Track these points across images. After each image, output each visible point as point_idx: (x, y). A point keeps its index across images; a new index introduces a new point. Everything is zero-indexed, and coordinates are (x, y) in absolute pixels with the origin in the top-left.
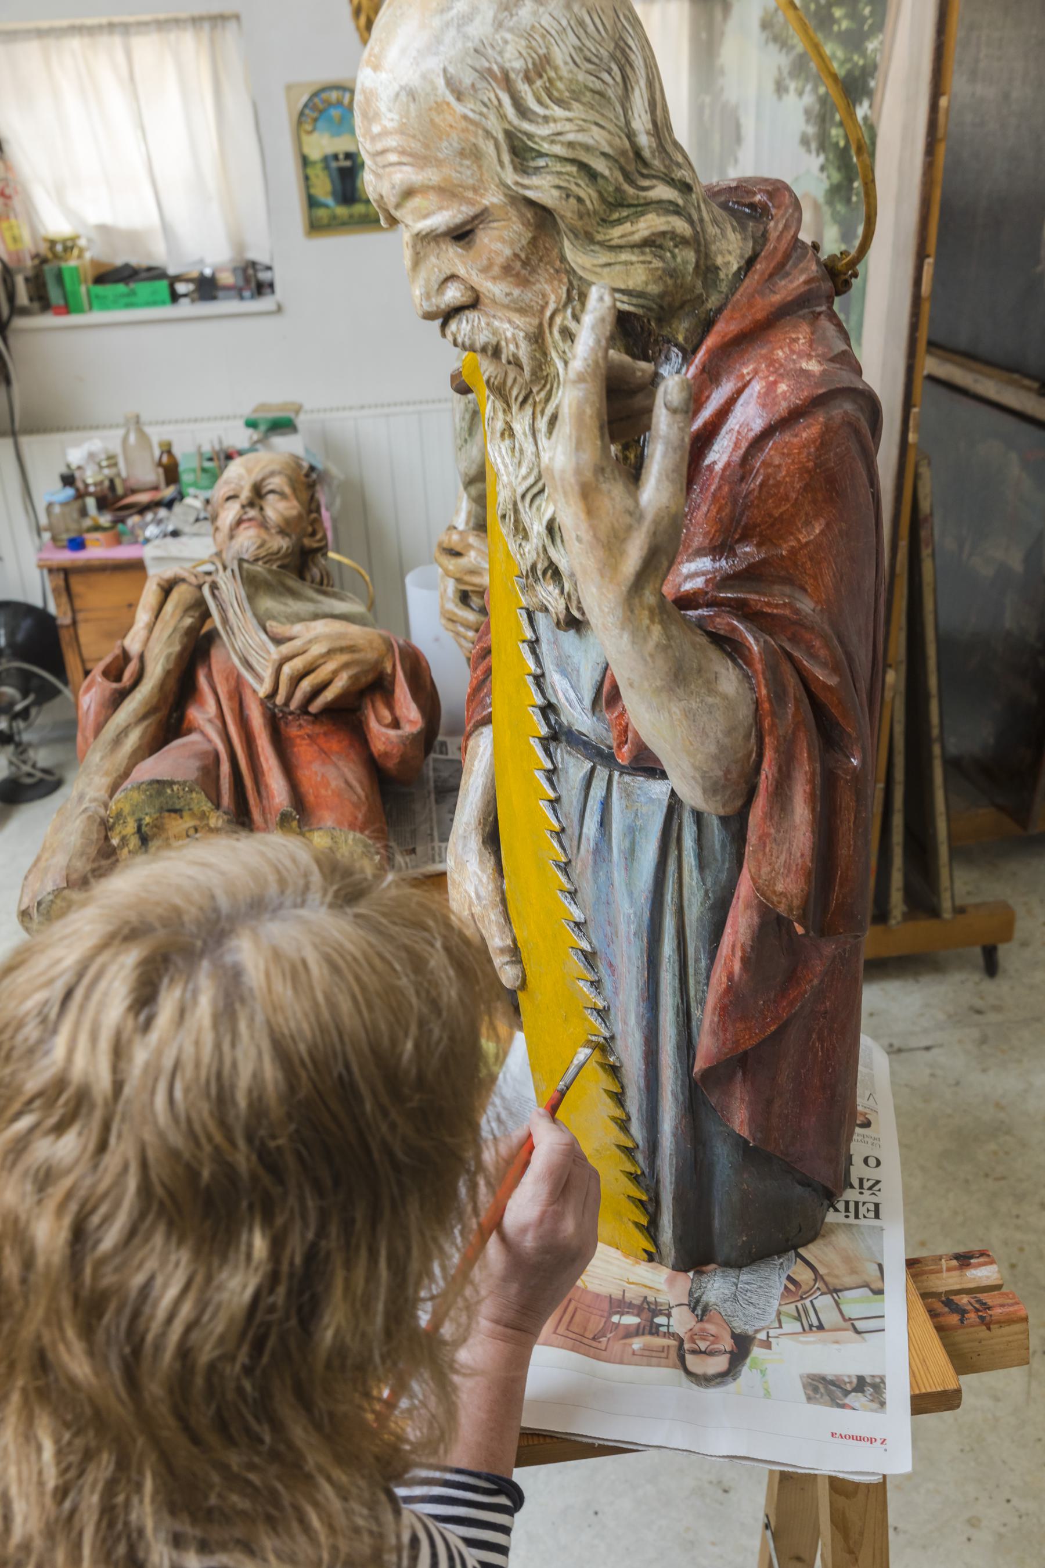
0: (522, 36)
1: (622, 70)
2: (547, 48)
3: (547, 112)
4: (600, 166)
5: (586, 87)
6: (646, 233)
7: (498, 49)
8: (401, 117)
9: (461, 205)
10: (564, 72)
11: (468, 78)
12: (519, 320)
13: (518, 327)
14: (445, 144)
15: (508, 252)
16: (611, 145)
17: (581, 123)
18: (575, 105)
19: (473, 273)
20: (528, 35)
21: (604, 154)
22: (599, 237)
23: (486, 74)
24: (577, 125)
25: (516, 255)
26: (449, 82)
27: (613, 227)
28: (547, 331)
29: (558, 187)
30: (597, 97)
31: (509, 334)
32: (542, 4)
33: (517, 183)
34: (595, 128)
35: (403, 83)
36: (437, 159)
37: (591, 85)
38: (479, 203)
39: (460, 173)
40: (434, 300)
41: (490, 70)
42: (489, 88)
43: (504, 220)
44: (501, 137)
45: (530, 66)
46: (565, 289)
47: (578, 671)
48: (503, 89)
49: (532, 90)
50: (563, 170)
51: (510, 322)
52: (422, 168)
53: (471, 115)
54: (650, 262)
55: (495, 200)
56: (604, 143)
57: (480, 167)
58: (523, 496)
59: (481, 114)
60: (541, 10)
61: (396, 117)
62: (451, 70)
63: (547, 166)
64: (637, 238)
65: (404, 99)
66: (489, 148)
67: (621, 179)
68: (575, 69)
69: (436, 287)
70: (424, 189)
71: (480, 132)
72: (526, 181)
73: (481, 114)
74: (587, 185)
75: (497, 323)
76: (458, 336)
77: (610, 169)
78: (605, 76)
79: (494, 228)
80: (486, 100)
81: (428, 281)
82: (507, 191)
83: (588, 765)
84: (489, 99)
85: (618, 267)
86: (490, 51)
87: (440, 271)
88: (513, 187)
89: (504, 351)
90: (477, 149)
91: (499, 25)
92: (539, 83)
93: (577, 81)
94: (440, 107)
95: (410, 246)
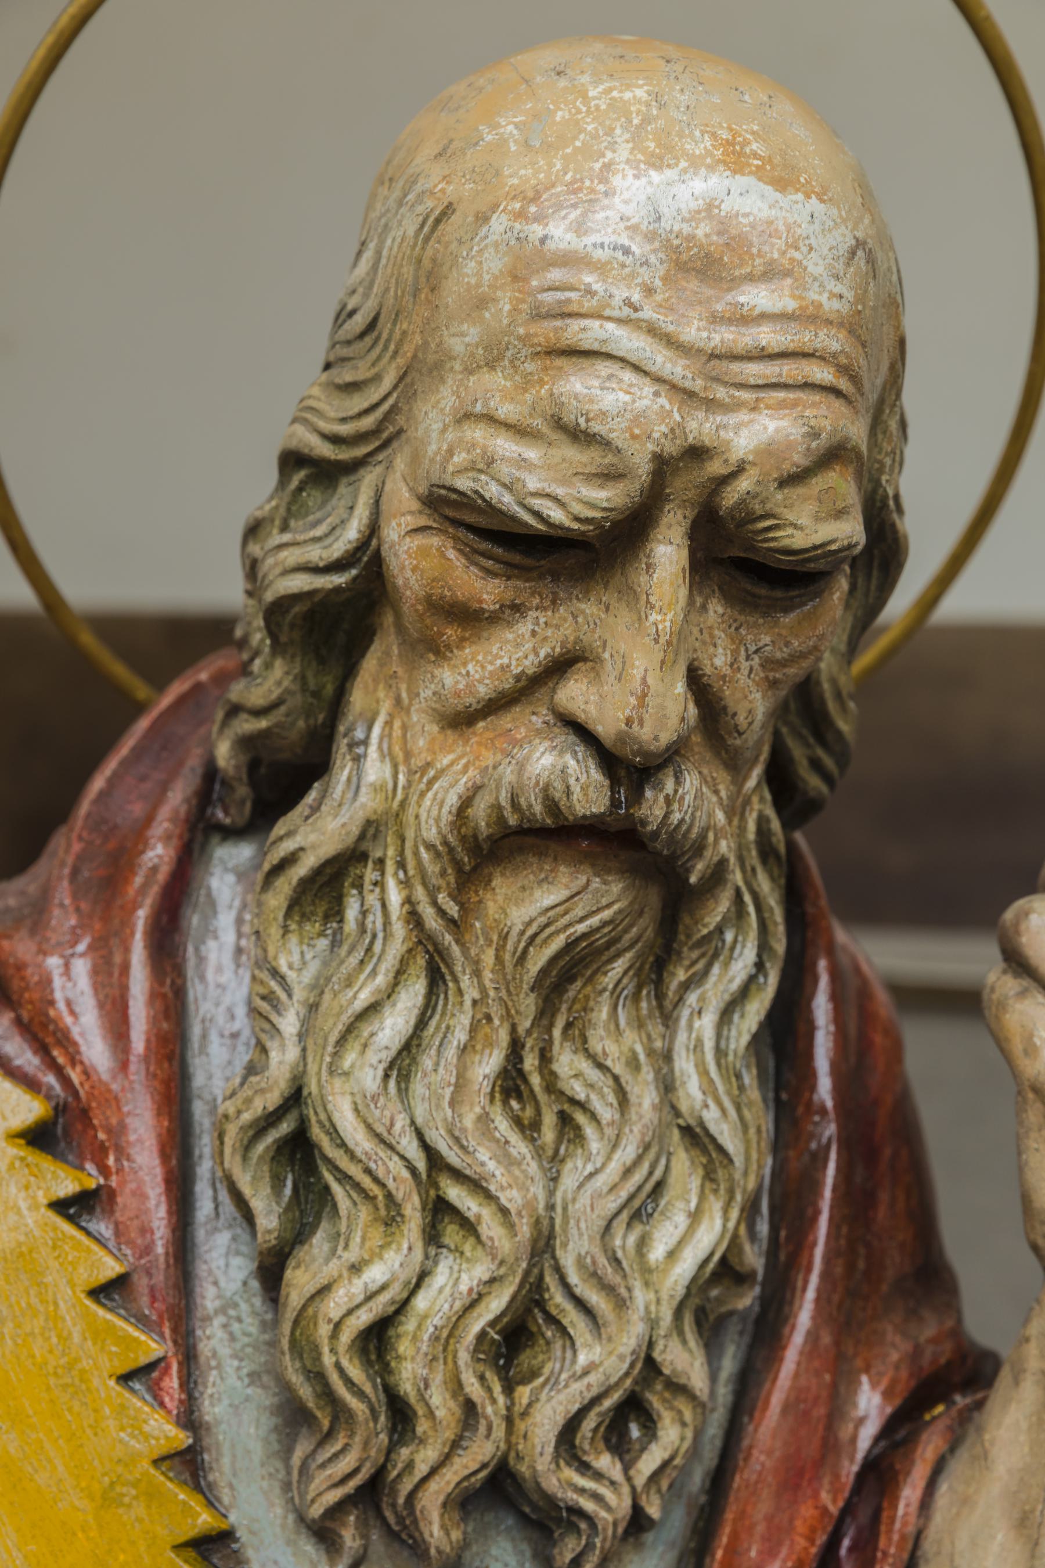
19: (745, 665)
75: (704, 789)
76: (676, 806)
89: (708, 853)
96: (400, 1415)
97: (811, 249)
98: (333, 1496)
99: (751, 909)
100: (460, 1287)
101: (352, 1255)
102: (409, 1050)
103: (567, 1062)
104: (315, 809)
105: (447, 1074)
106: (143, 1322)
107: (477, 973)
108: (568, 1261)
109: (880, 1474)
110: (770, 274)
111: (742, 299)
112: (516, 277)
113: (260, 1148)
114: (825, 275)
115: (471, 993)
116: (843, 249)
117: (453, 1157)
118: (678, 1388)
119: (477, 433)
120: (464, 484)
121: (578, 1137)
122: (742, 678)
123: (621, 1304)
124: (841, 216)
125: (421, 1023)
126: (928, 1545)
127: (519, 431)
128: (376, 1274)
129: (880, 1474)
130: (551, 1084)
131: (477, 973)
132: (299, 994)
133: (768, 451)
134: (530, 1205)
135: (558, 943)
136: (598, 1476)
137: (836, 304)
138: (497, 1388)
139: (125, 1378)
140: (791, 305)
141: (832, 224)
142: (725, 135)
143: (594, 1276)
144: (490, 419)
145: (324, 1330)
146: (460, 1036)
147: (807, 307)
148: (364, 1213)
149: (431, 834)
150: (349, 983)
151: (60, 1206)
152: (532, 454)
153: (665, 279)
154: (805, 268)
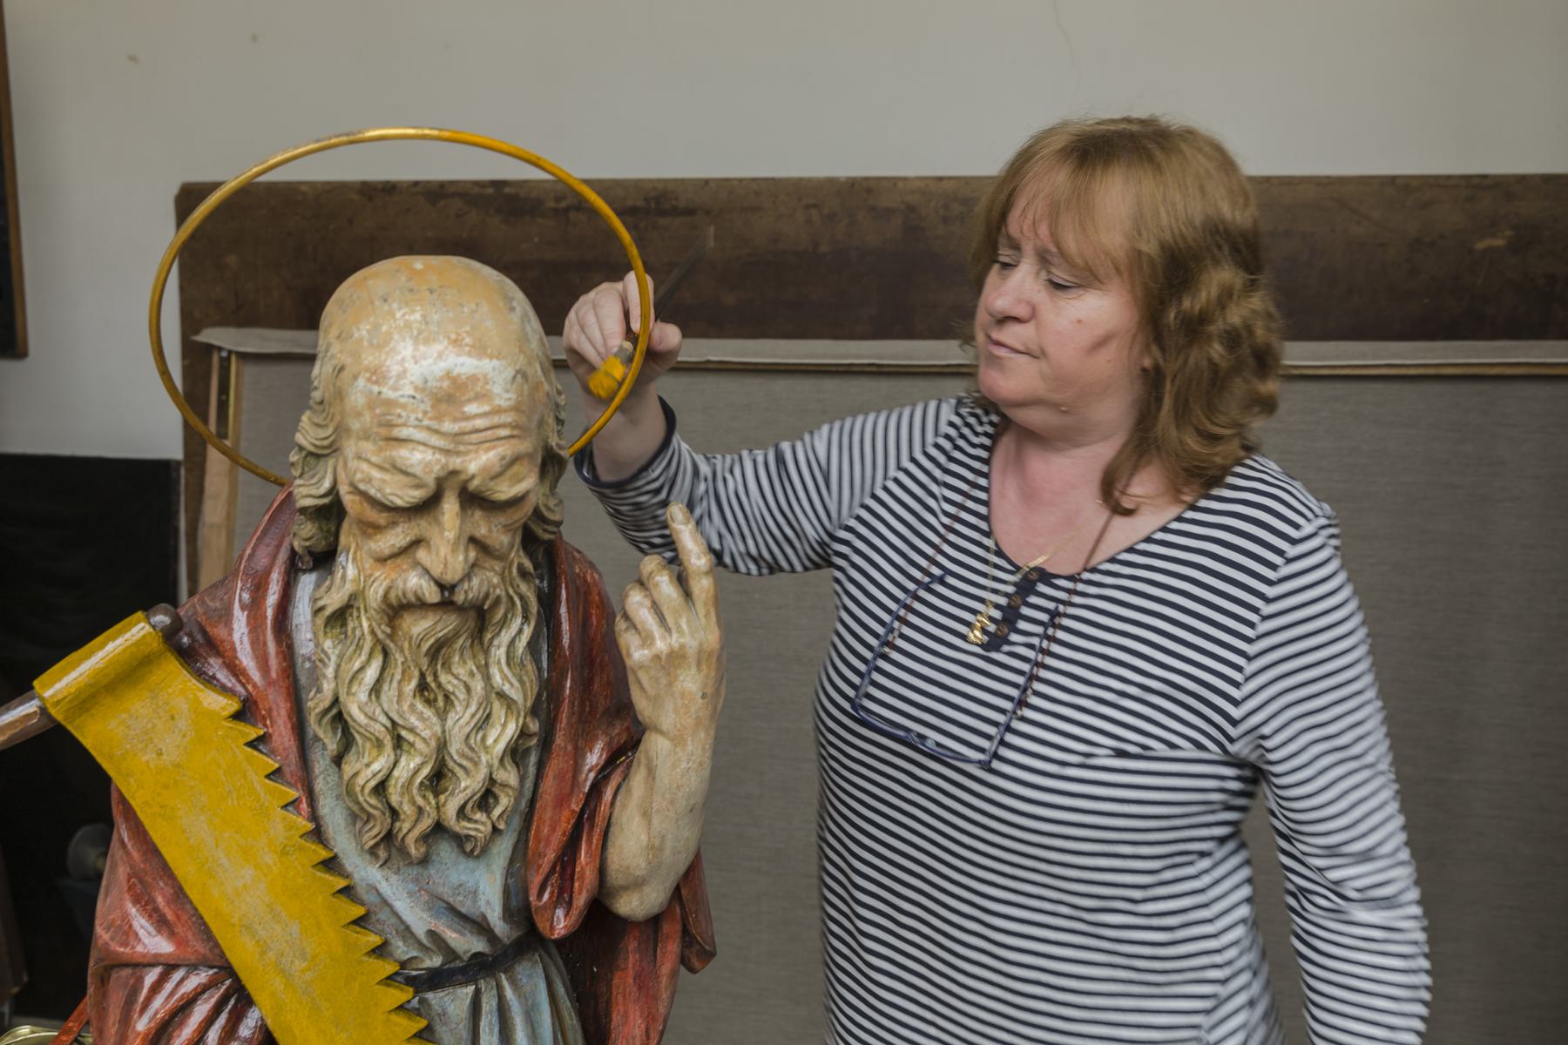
47: (475, 893)
58: (468, 736)
61: (513, 396)
83: (471, 989)
96: (395, 813)
98: (372, 843)
99: (518, 602)
100: (412, 766)
101: (366, 760)
102: (379, 681)
103: (443, 678)
104: (329, 589)
105: (394, 692)
106: (289, 785)
107: (402, 651)
108: (453, 751)
109: (597, 789)
110: (478, 397)
112: (371, 405)
113: (325, 720)
115: (400, 659)
117: (400, 721)
118: (504, 785)
119: (365, 466)
120: (362, 487)
121: (452, 704)
122: (495, 534)
123: (476, 764)
125: (381, 674)
126: (613, 820)
127: (381, 468)
128: (376, 766)
129: (597, 789)
130: (439, 686)
131: (402, 651)
132: (333, 658)
133: (484, 469)
134: (434, 734)
135: (432, 641)
136: (476, 822)
138: (431, 797)
139: (285, 807)
140: (487, 408)
142: (453, 336)
143: (463, 755)
144: (368, 461)
145: (358, 789)
146: (398, 677)
148: (368, 745)
149: (374, 605)
150: (351, 659)
151: (251, 744)
152: (387, 477)
153: (433, 406)
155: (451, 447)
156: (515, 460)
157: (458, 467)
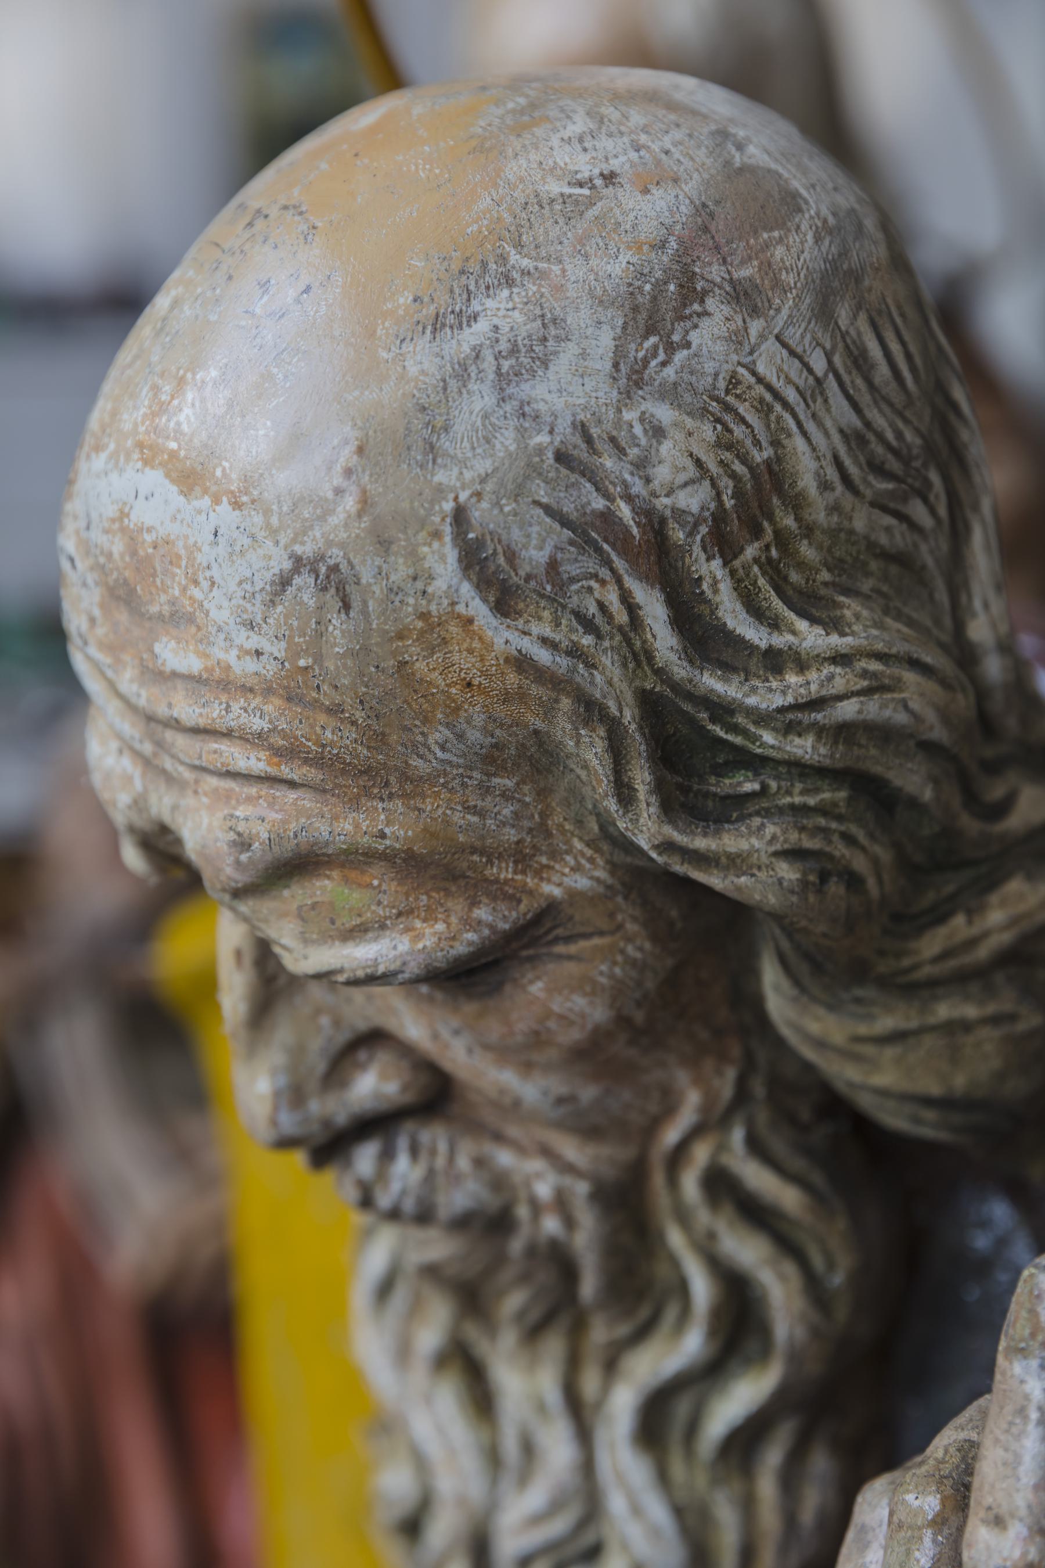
0: (705, 411)
1: (946, 479)
2: (776, 443)
3: (779, 641)
4: (912, 779)
5: (872, 546)
6: (1005, 938)
7: (633, 452)
8: (294, 653)
9: (474, 903)
10: (819, 515)
11: (536, 545)
12: (571, 1150)
13: (567, 1168)
14: (439, 734)
15: (599, 1014)
16: (945, 716)
17: (875, 666)
18: (850, 608)
20: (719, 406)
21: (929, 748)
22: (883, 967)
23: (590, 532)
24: (865, 674)
25: (622, 1021)
26: (474, 559)
27: (920, 931)
28: (658, 1179)
29: (794, 854)
30: (894, 569)
31: (544, 1190)
32: (755, 312)
33: (668, 847)
34: (910, 677)
35: (306, 549)
36: (405, 777)
37: (883, 540)
38: (531, 893)
39: (481, 813)
40: (315, 1106)
41: (607, 517)
42: (604, 573)
43: (601, 933)
44: (629, 716)
45: (729, 503)
46: (731, 1074)
48: (645, 578)
49: (733, 573)
50: (812, 801)
51: (547, 1152)
52: (354, 802)
53: (543, 656)
54: (1013, 1018)
55: (582, 883)
56: (931, 716)
57: (543, 794)
59: (574, 652)
60: (756, 326)
61: (278, 649)
62: (480, 513)
63: (764, 788)
64: (983, 953)
65: (309, 598)
66: (591, 753)
67: (956, 801)
68: (848, 501)
69: (321, 1067)
70: (353, 860)
71: (566, 703)
72: (700, 843)
73: (574, 652)
74: (871, 836)
75: (505, 1158)
77: (936, 781)
78: (918, 510)
79: (570, 958)
80: (593, 609)
81: (297, 1053)
82: (620, 857)
84: (602, 606)
85: (929, 1041)
86: (609, 463)
87: (337, 1023)
88: (654, 855)
90: (541, 744)
91: (632, 379)
92: (751, 551)
93: (851, 532)
94: (434, 629)
95: (248, 960)
97: (213, 583)
111: (158, 648)
114: (231, 622)
116: (264, 579)
124: (268, 525)
137: (251, 665)
140: (192, 664)
141: (247, 541)
147: (213, 670)
154: (207, 614)
155: (147, 748)
156: (294, 866)
157: (167, 819)
